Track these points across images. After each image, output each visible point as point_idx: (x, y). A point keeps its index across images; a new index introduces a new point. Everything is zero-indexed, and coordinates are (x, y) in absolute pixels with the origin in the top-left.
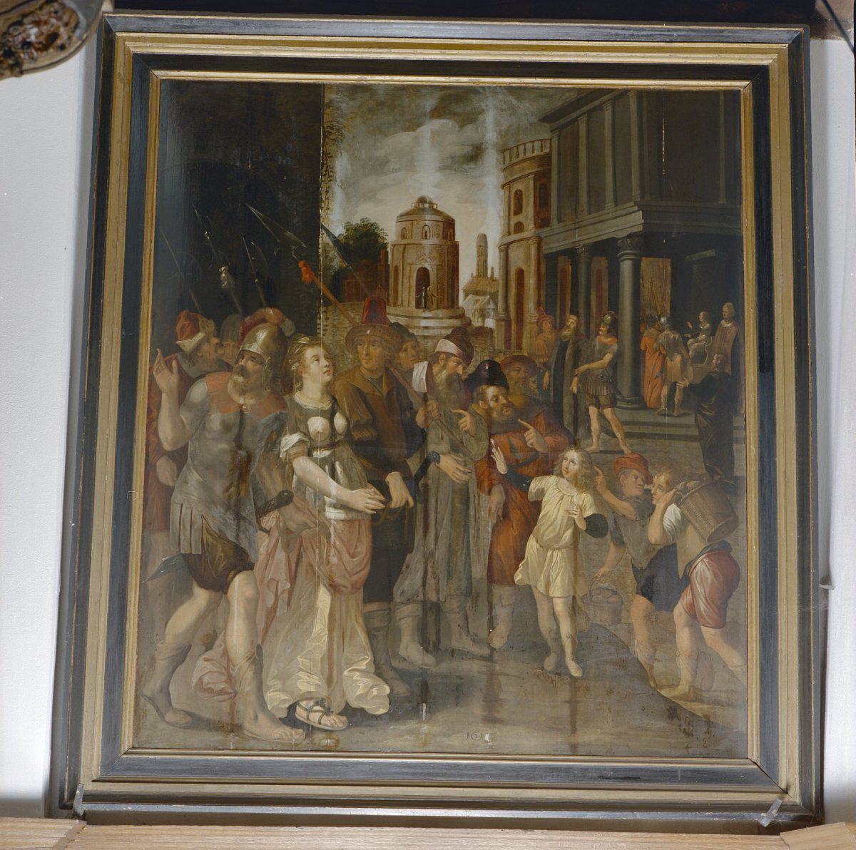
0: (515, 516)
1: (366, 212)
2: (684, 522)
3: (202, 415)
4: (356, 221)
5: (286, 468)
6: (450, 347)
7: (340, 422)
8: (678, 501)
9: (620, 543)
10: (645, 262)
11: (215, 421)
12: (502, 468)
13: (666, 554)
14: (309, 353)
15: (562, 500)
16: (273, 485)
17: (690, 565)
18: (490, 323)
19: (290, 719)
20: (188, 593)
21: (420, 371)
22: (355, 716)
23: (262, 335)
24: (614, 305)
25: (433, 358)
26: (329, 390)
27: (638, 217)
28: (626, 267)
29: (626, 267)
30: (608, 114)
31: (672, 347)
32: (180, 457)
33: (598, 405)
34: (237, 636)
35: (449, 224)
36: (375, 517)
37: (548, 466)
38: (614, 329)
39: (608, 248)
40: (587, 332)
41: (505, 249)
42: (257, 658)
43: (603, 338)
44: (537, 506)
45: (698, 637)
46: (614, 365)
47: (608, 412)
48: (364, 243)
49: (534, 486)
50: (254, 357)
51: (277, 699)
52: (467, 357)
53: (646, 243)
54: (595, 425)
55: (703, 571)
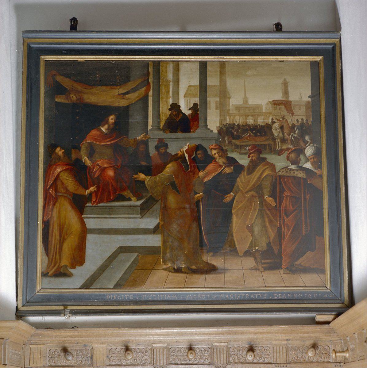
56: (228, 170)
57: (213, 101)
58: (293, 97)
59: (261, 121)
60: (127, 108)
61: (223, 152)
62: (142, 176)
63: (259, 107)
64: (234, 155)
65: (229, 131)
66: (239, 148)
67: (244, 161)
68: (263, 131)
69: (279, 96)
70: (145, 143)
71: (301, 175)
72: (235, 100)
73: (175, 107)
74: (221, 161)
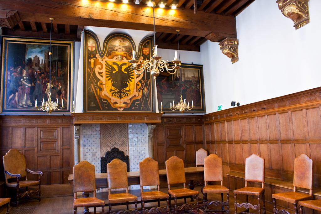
0: (45, 87)
1: (30, 57)
2: (61, 88)
3: (13, 77)
4: (29, 58)
5: (22, 82)
6: (39, 70)
7: (27, 77)
8: (61, 85)
9: (55, 89)
10: (59, 62)
11: (14, 77)
12: (44, 82)
13: (60, 90)
14: (24, 71)
15: (49, 85)
16: (20, 84)
17: (62, 92)
18: (43, 68)
20: (11, 94)
21: (35, 73)
22: (29, 106)
23: (19, 69)
24: (55, 67)
26: (26, 74)
27: (58, 58)
28: (57, 63)
29: (57, 63)
30: (55, 48)
31: (61, 71)
32: (10, 81)
33: (54, 76)
34: (17, 99)
35: (39, 58)
36: (31, 87)
37: (48, 82)
38: (55, 69)
41: (44, 61)
42: (19, 101)
43: (54, 70)
44: (47, 86)
46: (55, 72)
47: (54, 77)
48: (30, 59)
49: (47, 84)
50: (18, 71)
51: (20, 104)
52: (40, 71)
53: (59, 61)
54: (53, 78)
55: (63, 92)
56: (185, 88)
57: (183, 76)
58: (195, 76)
59: (190, 80)
61: (185, 85)
62: (171, 89)
63: (190, 77)
64: (186, 86)
67: (188, 87)
68: (191, 81)
69: (193, 75)
71: (197, 89)
72: (186, 76)
73: (176, 76)
74: (184, 86)
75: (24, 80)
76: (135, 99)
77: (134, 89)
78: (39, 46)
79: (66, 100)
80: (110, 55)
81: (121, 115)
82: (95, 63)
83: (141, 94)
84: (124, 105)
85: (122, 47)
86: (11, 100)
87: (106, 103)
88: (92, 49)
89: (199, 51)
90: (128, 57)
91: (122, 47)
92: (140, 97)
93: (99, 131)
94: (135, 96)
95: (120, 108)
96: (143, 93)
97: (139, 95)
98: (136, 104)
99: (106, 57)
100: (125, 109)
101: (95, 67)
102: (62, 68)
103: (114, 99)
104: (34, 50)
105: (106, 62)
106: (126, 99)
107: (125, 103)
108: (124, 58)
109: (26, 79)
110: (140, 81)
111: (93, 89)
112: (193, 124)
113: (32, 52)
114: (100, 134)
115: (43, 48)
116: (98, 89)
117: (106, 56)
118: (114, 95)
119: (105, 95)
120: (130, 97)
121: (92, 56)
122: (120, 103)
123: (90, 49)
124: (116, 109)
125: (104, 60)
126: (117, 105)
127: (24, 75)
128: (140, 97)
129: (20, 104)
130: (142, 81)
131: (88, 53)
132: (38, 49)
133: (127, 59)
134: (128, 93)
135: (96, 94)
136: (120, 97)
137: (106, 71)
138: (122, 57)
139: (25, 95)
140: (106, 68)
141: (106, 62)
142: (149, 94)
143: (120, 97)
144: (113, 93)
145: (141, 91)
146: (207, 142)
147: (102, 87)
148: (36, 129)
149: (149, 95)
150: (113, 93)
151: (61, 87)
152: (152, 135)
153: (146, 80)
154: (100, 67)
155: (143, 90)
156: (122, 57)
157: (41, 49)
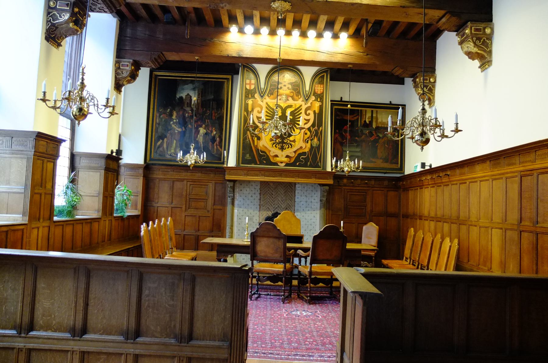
1: (181, 95)
3: (162, 119)
5: (171, 126)
11: (163, 120)
15: (202, 131)
16: (169, 128)
19: (171, 155)
21: (187, 114)
24: (210, 107)
25: (188, 113)
26: (176, 117)
32: (159, 124)
34: (165, 146)
37: (201, 126)
39: (209, 100)
40: (206, 110)
45: (217, 147)
48: (181, 98)
51: (169, 153)
53: (213, 100)
55: (218, 139)
57: (374, 120)
60: (354, 121)
61: (376, 133)
65: (378, 128)
66: (380, 133)
67: (381, 136)
70: (358, 130)
72: (379, 120)
73: (365, 121)
75: (174, 123)
76: (301, 151)
77: (300, 140)
78: (192, 82)
79: (220, 149)
80: (272, 94)
81: (281, 172)
82: (253, 105)
83: (309, 145)
84: (286, 160)
85: (289, 84)
86: (159, 147)
87: (264, 156)
88: (250, 87)
89: (403, 84)
90: (295, 97)
91: (289, 84)
92: (307, 150)
93: (259, 191)
94: (301, 147)
95: (281, 163)
96: (311, 145)
97: (307, 148)
98: (302, 158)
99: (267, 97)
100: (287, 165)
101: (253, 110)
102: (217, 109)
103: (274, 151)
104: (186, 86)
105: (267, 103)
106: (289, 151)
107: (287, 156)
108: (290, 99)
109: (176, 123)
110: (309, 129)
111: (250, 137)
112: (385, 188)
113: (183, 89)
114: (260, 194)
115: (197, 84)
116: (256, 138)
117: (268, 95)
118: (274, 145)
119: (263, 145)
120: (294, 149)
121: (250, 96)
122: (281, 157)
123: (248, 87)
124: (276, 164)
125: (265, 101)
126: (278, 159)
127: (174, 117)
128: (307, 150)
129: (169, 153)
130: (311, 128)
131: (246, 92)
132: (191, 86)
133: (293, 99)
134: (292, 143)
135: (252, 145)
136: (282, 149)
137: (267, 115)
138: (287, 96)
139: (175, 141)
140: (266, 112)
141: (267, 103)
142: (319, 145)
143: (282, 149)
144: (274, 144)
145: (309, 142)
146: (403, 215)
147: (260, 135)
148: (185, 182)
149: (319, 147)
150: (274, 144)
151: (215, 132)
152: (325, 199)
153: (316, 127)
154: (259, 109)
155: (311, 140)
156: (287, 96)
157: (194, 86)
